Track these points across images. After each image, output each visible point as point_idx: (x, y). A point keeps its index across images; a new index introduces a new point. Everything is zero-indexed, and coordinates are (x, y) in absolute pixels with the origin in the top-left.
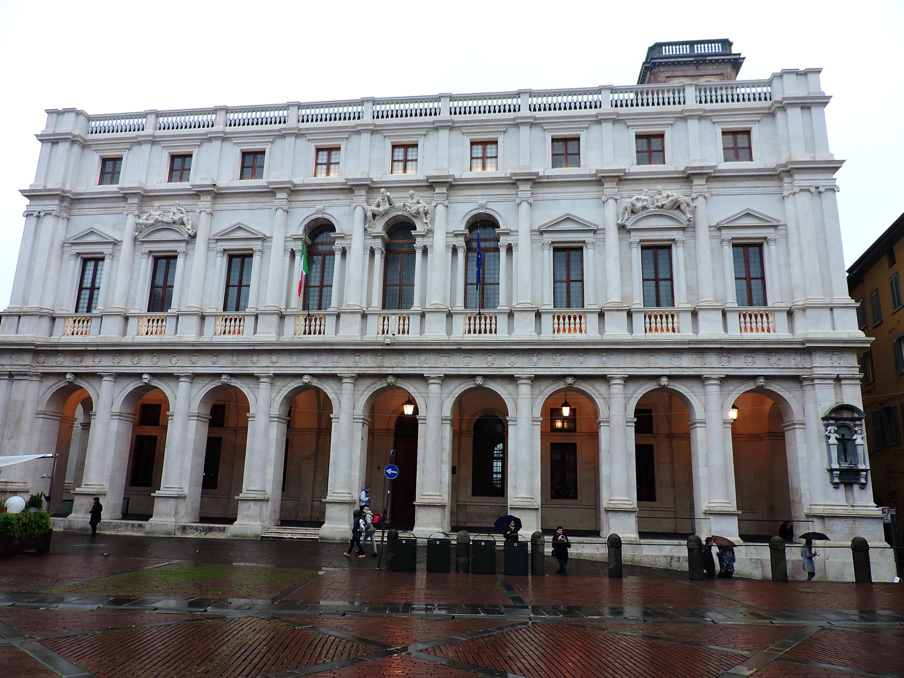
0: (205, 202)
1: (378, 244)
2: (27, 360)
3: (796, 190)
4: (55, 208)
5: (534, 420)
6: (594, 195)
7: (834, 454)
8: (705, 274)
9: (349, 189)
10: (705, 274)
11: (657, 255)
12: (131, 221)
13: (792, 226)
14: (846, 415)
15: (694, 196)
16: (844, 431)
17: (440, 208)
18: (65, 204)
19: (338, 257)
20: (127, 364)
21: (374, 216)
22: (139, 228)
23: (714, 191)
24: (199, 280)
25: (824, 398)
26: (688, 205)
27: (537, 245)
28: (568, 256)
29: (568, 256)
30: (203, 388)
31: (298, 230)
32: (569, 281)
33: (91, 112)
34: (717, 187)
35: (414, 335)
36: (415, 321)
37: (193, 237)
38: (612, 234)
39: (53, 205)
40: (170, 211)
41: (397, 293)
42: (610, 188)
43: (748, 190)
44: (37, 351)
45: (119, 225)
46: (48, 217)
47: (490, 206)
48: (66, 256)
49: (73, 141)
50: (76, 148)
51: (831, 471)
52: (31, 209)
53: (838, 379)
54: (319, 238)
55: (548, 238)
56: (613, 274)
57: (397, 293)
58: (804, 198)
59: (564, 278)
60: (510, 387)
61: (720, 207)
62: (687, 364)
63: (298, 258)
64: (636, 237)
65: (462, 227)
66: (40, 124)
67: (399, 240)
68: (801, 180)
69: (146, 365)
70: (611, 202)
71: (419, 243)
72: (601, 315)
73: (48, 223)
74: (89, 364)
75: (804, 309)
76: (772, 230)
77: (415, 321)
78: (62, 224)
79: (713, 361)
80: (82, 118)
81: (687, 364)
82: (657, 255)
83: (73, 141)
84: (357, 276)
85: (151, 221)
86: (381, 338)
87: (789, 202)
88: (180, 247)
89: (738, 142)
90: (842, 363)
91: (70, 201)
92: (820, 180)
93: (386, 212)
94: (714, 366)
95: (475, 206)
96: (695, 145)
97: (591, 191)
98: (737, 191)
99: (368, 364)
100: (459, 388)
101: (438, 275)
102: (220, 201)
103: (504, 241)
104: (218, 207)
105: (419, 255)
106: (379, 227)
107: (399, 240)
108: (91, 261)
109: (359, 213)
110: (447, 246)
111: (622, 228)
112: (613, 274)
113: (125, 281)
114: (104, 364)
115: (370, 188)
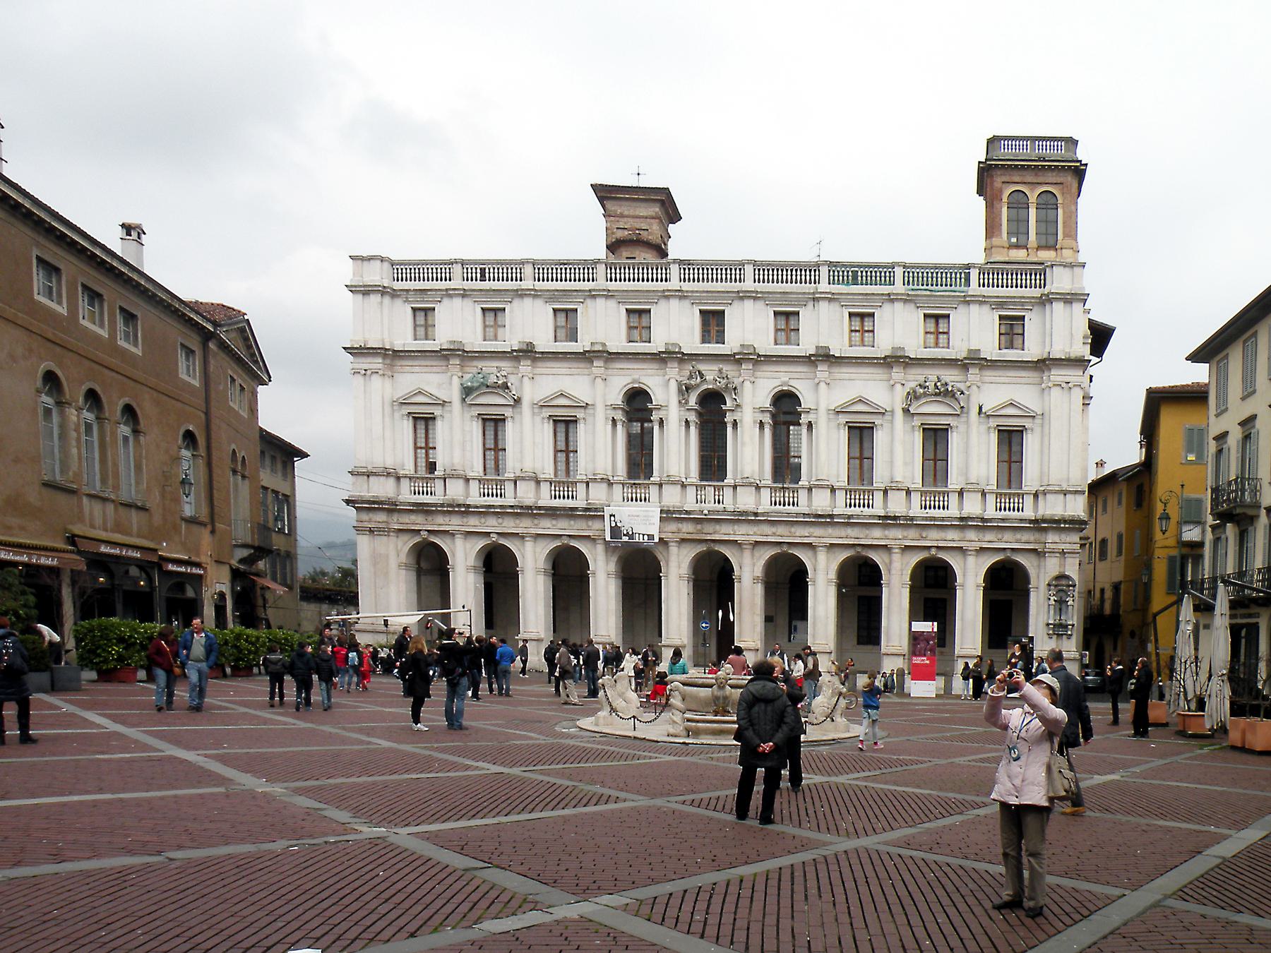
0: (525, 367)
1: (692, 417)
2: (381, 517)
3: (1050, 384)
4: (380, 366)
5: (830, 581)
6: (885, 376)
7: (1052, 612)
8: (974, 456)
9: (662, 358)
10: (974, 456)
11: (936, 438)
12: (456, 382)
13: (1046, 415)
14: (1064, 582)
15: (968, 384)
16: (1061, 594)
17: (747, 384)
18: (388, 361)
19: (656, 428)
20: (474, 524)
21: (687, 389)
22: (467, 391)
23: (987, 379)
24: (529, 444)
25: (1052, 566)
26: (962, 393)
27: (833, 424)
28: (861, 435)
29: (861, 435)
30: (547, 547)
31: (618, 399)
32: (861, 458)
33: (394, 257)
34: (989, 375)
35: (728, 503)
36: (728, 493)
37: (518, 401)
38: (899, 414)
39: (377, 363)
40: (493, 371)
41: (713, 463)
42: (897, 373)
43: (1014, 380)
44: (392, 507)
45: (442, 384)
46: (375, 376)
47: (792, 383)
48: (397, 415)
49: (383, 291)
50: (387, 299)
51: (1048, 625)
52: (356, 366)
53: (1063, 553)
54: (637, 404)
55: (843, 419)
56: (898, 454)
57: (713, 463)
58: (1056, 392)
59: (858, 455)
60: (810, 553)
61: (993, 393)
62: (952, 538)
63: (619, 427)
64: (917, 421)
65: (767, 404)
66: (347, 273)
67: (712, 414)
68: (1057, 375)
69: (491, 525)
70: (898, 386)
71: (729, 418)
72: (885, 492)
73: (376, 381)
74: (441, 522)
75: (1044, 493)
76: (1030, 420)
77: (728, 493)
78: (388, 382)
79: (971, 535)
80: (386, 265)
81: (952, 538)
82: (936, 438)
83: (383, 291)
84: (676, 448)
85: (476, 384)
86: (696, 507)
87: (1046, 392)
88: (508, 412)
89: (1012, 329)
90: (1068, 540)
91: (393, 356)
92: (1073, 375)
93: (698, 386)
94: (972, 539)
95: (777, 382)
96: (975, 330)
97: (878, 373)
98: (1006, 380)
99: (687, 528)
100: (768, 553)
101: (749, 450)
102: (539, 364)
103: (804, 419)
104: (538, 371)
105: (729, 430)
106: (693, 400)
107: (712, 414)
108: (424, 422)
109: (673, 386)
110: (755, 422)
111: (906, 411)
112: (898, 454)
113: (459, 441)
114: (453, 523)
115: (684, 358)
